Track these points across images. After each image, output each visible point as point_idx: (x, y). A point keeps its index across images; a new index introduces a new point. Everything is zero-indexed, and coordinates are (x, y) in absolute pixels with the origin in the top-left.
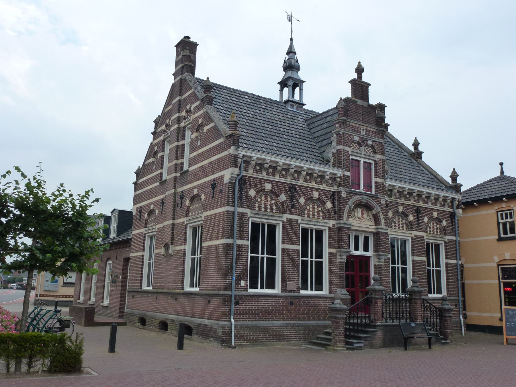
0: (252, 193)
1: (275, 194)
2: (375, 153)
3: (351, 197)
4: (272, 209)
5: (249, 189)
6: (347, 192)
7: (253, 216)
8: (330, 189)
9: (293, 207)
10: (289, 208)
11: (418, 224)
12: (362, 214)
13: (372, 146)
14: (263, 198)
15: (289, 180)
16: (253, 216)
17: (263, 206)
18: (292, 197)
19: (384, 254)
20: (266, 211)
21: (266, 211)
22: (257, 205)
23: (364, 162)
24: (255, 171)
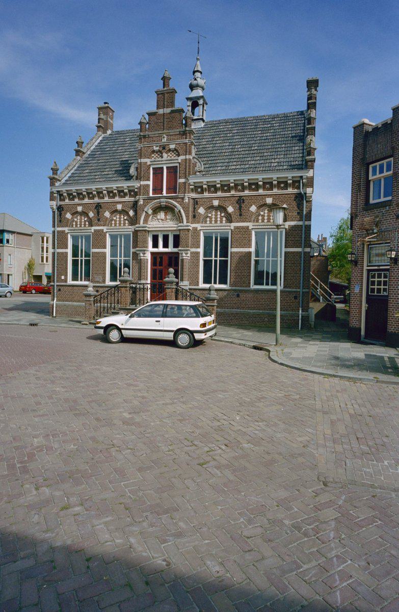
0: (68, 216)
1: (84, 214)
2: (179, 155)
3: (148, 203)
4: (85, 225)
5: (66, 213)
6: (144, 200)
7: (70, 231)
8: (132, 199)
9: (99, 220)
10: (96, 221)
11: (241, 215)
12: (165, 215)
13: (175, 149)
14: (79, 218)
15: (96, 200)
16: (70, 231)
17: (78, 223)
18: (98, 213)
19: (183, 249)
20: (81, 226)
21: (81, 226)
22: (74, 223)
23: (167, 167)
24: (70, 199)
